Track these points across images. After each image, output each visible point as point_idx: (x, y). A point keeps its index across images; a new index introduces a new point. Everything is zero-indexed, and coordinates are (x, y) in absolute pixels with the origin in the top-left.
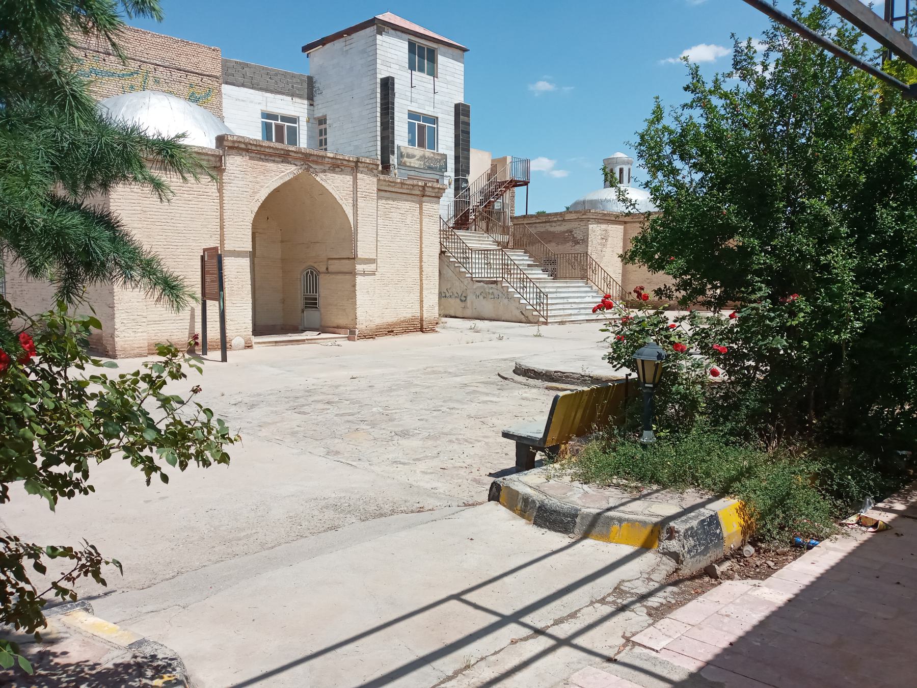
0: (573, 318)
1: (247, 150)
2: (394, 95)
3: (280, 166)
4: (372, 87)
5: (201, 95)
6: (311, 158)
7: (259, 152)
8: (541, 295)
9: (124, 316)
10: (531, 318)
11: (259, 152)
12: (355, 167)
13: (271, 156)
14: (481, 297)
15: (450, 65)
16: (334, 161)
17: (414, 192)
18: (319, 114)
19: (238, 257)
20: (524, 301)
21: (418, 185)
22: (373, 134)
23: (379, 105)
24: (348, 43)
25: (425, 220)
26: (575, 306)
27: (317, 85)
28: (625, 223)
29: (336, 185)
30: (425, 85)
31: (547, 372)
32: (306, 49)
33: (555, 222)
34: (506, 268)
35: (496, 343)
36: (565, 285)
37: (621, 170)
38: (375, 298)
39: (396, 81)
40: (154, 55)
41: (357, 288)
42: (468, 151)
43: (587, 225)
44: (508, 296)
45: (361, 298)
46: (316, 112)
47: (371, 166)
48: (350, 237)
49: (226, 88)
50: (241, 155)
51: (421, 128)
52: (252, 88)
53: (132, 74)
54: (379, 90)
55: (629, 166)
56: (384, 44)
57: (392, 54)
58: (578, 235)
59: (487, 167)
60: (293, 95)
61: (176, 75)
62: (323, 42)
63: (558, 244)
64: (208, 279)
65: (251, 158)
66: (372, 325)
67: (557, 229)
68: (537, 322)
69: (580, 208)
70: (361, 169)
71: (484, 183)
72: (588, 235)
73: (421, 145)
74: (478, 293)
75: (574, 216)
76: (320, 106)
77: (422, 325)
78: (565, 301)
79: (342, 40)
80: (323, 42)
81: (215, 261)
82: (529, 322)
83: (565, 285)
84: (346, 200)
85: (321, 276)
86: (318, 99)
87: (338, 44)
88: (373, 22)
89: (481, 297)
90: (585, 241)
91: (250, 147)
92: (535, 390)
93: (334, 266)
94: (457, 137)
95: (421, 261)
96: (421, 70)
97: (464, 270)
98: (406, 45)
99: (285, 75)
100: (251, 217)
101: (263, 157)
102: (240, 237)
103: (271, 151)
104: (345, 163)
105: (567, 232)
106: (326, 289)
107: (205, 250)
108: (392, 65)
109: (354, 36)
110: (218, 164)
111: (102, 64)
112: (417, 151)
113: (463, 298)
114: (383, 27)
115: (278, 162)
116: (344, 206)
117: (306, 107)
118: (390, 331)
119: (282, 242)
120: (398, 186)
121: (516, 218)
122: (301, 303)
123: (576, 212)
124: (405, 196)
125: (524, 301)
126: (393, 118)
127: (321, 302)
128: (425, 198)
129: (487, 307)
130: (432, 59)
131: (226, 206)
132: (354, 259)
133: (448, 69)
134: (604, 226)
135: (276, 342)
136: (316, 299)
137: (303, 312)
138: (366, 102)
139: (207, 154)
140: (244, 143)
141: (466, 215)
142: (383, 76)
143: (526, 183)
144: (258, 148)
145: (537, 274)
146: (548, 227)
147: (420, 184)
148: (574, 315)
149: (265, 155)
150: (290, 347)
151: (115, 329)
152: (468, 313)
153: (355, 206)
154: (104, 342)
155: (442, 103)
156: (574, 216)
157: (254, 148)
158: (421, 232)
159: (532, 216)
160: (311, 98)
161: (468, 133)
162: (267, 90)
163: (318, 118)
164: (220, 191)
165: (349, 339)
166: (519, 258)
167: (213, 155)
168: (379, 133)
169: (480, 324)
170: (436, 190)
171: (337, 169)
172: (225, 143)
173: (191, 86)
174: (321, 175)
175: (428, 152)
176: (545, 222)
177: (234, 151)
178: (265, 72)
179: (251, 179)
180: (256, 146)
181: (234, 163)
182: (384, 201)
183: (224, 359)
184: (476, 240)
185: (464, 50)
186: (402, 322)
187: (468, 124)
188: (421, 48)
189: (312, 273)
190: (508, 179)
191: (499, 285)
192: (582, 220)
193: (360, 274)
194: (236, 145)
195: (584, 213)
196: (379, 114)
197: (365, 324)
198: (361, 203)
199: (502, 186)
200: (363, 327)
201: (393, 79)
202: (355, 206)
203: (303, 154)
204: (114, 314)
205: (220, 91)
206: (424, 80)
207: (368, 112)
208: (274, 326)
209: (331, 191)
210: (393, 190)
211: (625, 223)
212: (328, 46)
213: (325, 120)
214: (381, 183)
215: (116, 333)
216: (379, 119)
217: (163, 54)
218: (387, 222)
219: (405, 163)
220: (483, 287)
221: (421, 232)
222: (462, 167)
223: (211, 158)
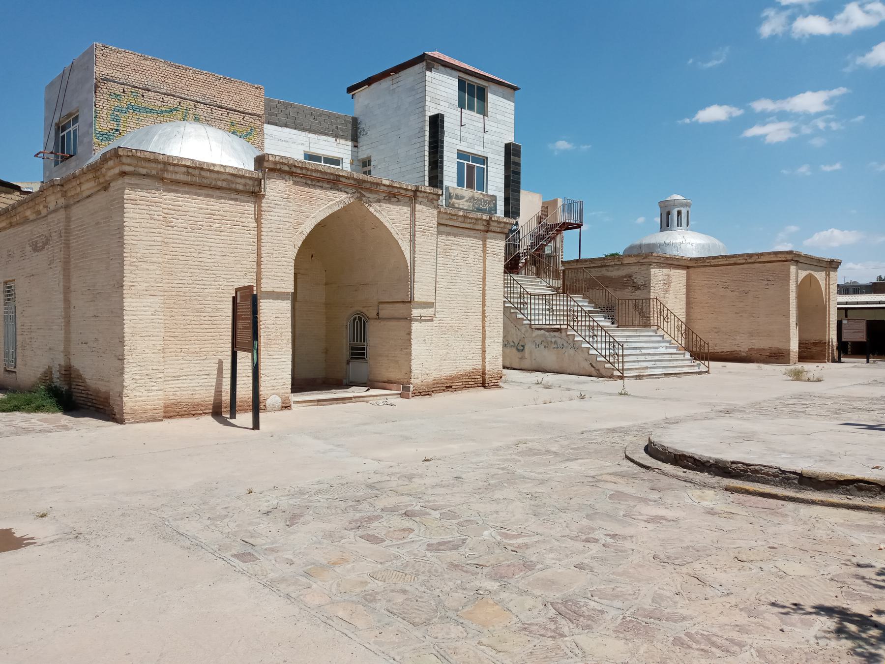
0: (649, 372)
1: (291, 174)
2: (443, 132)
3: (329, 193)
4: (421, 125)
5: (242, 125)
7: (305, 176)
8: (613, 344)
9: (136, 370)
10: (603, 372)
12: (413, 196)
13: (319, 181)
14: (542, 347)
15: (501, 104)
17: (477, 227)
18: (363, 155)
19: (277, 299)
20: (594, 352)
21: (481, 219)
22: (421, 174)
23: (427, 143)
24: (394, 81)
25: (489, 258)
26: (649, 358)
27: (362, 126)
28: (688, 267)
29: (392, 217)
30: (475, 123)
31: (717, 462)
32: (350, 90)
33: (612, 266)
34: (571, 315)
35: (577, 403)
36: (634, 334)
37: (679, 213)
38: (433, 347)
39: (445, 119)
40: (194, 92)
41: (413, 336)
42: (519, 192)
43: (648, 270)
44: (576, 346)
45: (417, 347)
46: (360, 154)
47: (431, 196)
48: (406, 278)
49: (268, 129)
50: (283, 178)
51: (470, 168)
52: (295, 129)
53: (171, 110)
54: (427, 128)
55: (688, 208)
56: (434, 81)
57: (441, 91)
58: (639, 280)
59: (537, 209)
60: (337, 136)
61: (217, 112)
62: (369, 82)
63: (615, 290)
64: (240, 325)
65: (295, 183)
66: (429, 380)
67: (615, 273)
68: (611, 376)
69: (635, 252)
70: (420, 199)
71: (534, 225)
72: (650, 280)
73: (470, 185)
74: (538, 342)
75: (633, 260)
76: (364, 148)
77: (484, 380)
78: (638, 352)
79: (388, 78)
80: (369, 82)
81: (249, 303)
82: (602, 377)
83: (634, 334)
85: (371, 322)
86: (363, 140)
87: (385, 83)
89: (542, 347)
90: (646, 286)
91: (294, 170)
92: (710, 493)
93: (386, 311)
94: (507, 178)
95: (484, 305)
96: (471, 108)
97: (521, 316)
98: (455, 83)
99: (329, 115)
100: (293, 252)
101: (309, 182)
102: (280, 276)
103: (319, 175)
104: (402, 192)
105: (625, 277)
106: (378, 337)
107: (237, 290)
108: (442, 103)
110: (257, 189)
111: (140, 99)
112: (466, 192)
113: (529, 350)
114: (431, 63)
115: (326, 189)
116: (400, 242)
117: (350, 148)
118: (448, 386)
119: (326, 284)
120: (460, 219)
121: (568, 262)
122: (346, 353)
123: (636, 256)
124: (467, 231)
125: (594, 352)
126: (442, 157)
127: (370, 352)
128: (489, 234)
129: (549, 357)
130: (482, 95)
131: (265, 239)
132: (410, 302)
133: (498, 107)
134: (666, 271)
135: (318, 401)
136: (363, 349)
137: (348, 363)
138: (414, 141)
139: (243, 177)
140: (288, 165)
141: (517, 259)
142: (432, 114)
143: (579, 226)
144: (304, 172)
145: (601, 320)
146: (604, 272)
147: (484, 217)
148: (651, 368)
149: (312, 180)
150: (334, 406)
151: (124, 387)
152: (526, 364)
153: (412, 241)
154: (112, 402)
155: (492, 143)
156: (633, 260)
157: (299, 171)
158: (484, 273)
159: (586, 260)
160: (355, 139)
161: (519, 173)
162: (310, 131)
163: (363, 159)
164: (258, 220)
165: (402, 396)
166: (581, 302)
167: (250, 178)
168: (427, 173)
169: (549, 378)
170: (502, 225)
171: (393, 199)
172: (266, 164)
173: (232, 124)
174: (375, 205)
175: (477, 194)
176: (601, 266)
177: (275, 175)
178: (308, 112)
179: (295, 208)
180: (301, 168)
181: (276, 189)
182: (444, 237)
183: (256, 426)
184: (534, 285)
185: (515, 89)
187: (519, 165)
188: (471, 86)
189: (360, 319)
190: (560, 219)
191: (564, 334)
192: (642, 264)
193: (417, 320)
194: (278, 167)
195: (645, 257)
196: (427, 153)
197: (421, 379)
198: (419, 239)
199: (551, 230)
200: (419, 382)
201: (442, 116)
202: (412, 241)
203: (355, 180)
204: (123, 368)
205: (262, 130)
206: (474, 118)
207: (416, 151)
208: (314, 380)
209: (386, 224)
211: (688, 267)
212: (374, 86)
213: (370, 161)
214: (442, 215)
215: (125, 391)
216: (427, 158)
217: (204, 91)
218: (447, 261)
219: (453, 204)
220: (543, 335)
221: (484, 273)
222: (512, 208)
223: (248, 181)
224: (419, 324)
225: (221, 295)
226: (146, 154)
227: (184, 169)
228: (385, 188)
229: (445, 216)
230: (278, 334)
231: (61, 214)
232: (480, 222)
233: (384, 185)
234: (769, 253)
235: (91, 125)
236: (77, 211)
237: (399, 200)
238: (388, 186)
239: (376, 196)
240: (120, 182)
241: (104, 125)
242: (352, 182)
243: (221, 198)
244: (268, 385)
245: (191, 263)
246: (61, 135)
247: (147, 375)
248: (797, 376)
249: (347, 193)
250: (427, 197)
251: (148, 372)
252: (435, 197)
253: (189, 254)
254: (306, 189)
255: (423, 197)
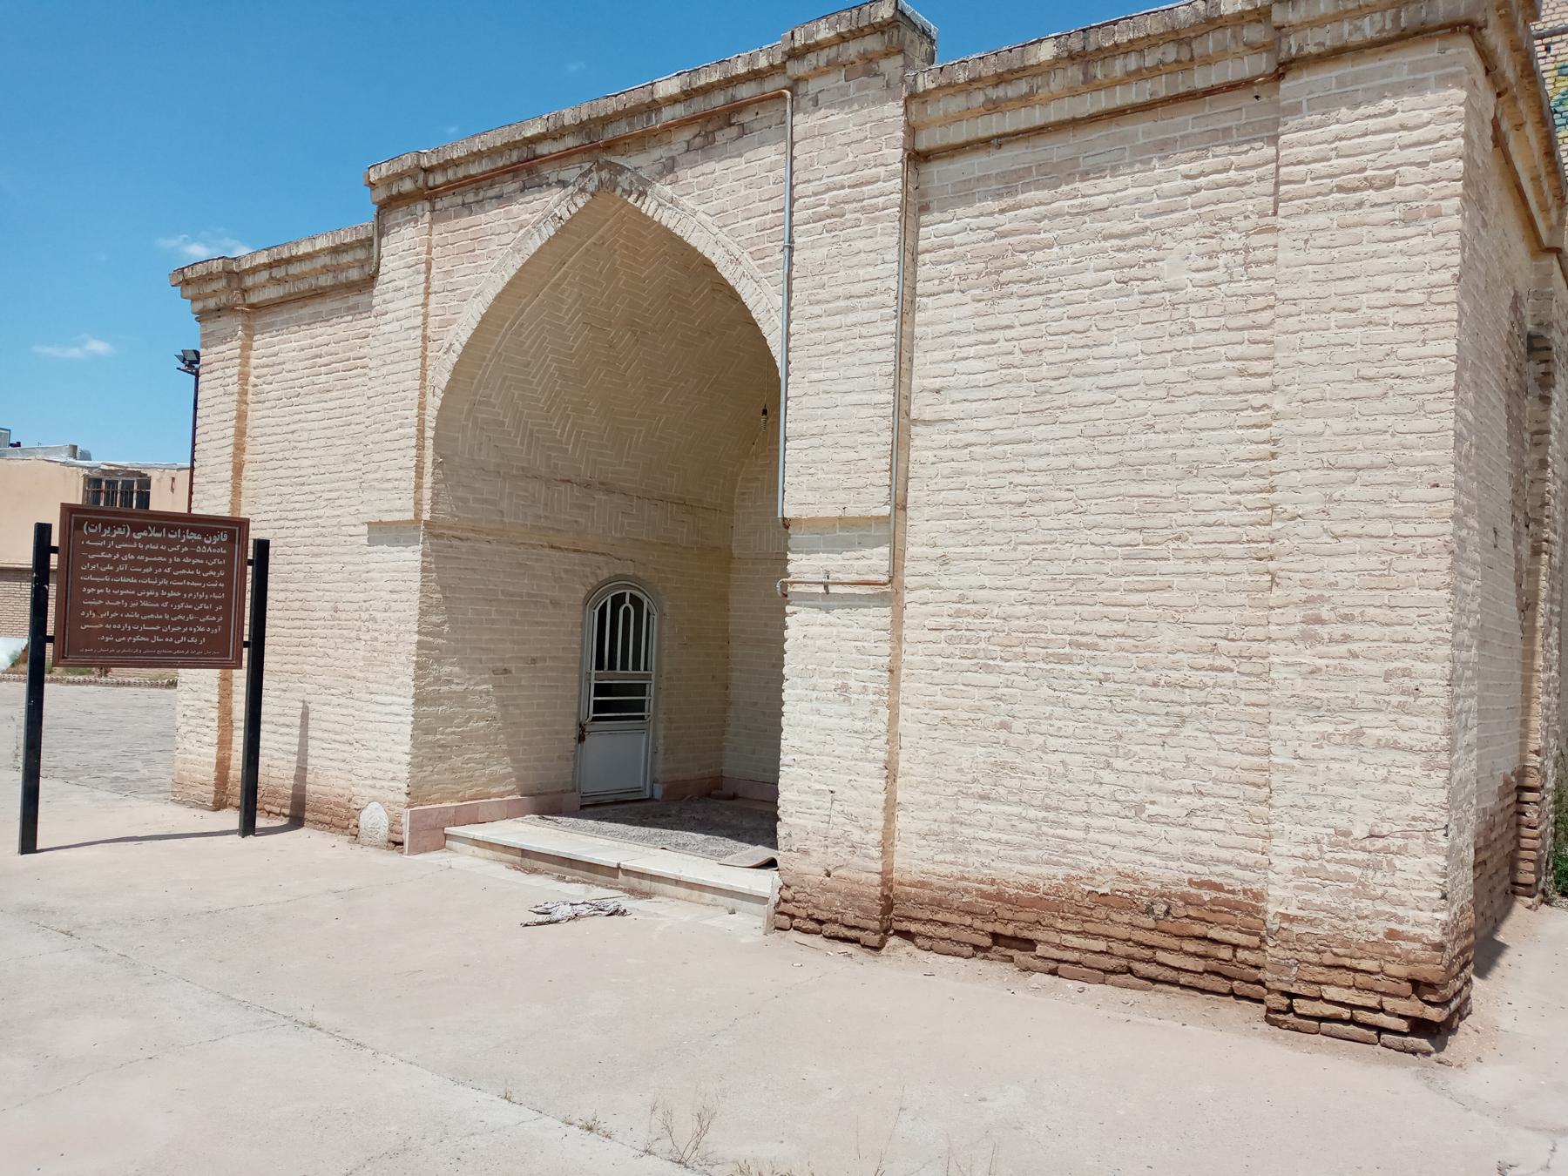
3: (515, 208)
6: (609, 134)
7: (453, 187)
11: (453, 187)
16: (699, 105)
65: (437, 216)
84: (759, 255)
103: (485, 166)
104: (745, 92)
120: (1057, 83)
124: (1140, 129)
135: (525, 853)
144: (450, 174)
157: (439, 179)
171: (721, 137)
186: (1124, 903)
210: (1037, 117)
214: (936, 110)
224: (821, 616)
225: (319, 540)
226: (198, 267)
227: (265, 275)
228: (679, 111)
229: (956, 104)
230: (392, 637)
232: (1211, 43)
233: (673, 100)
237: (744, 130)
238: (688, 95)
239: (660, 153)
242: (570, 142)
243: (334, 313)
244: (366, 773)
245: (282, 472)
247: (200, 710)
249: (563, 184)
250: (832, 65)
251: (199, 704)
252: (873, 43)
253: (280, 456)
254: (465, 221)
255: (818, 72)
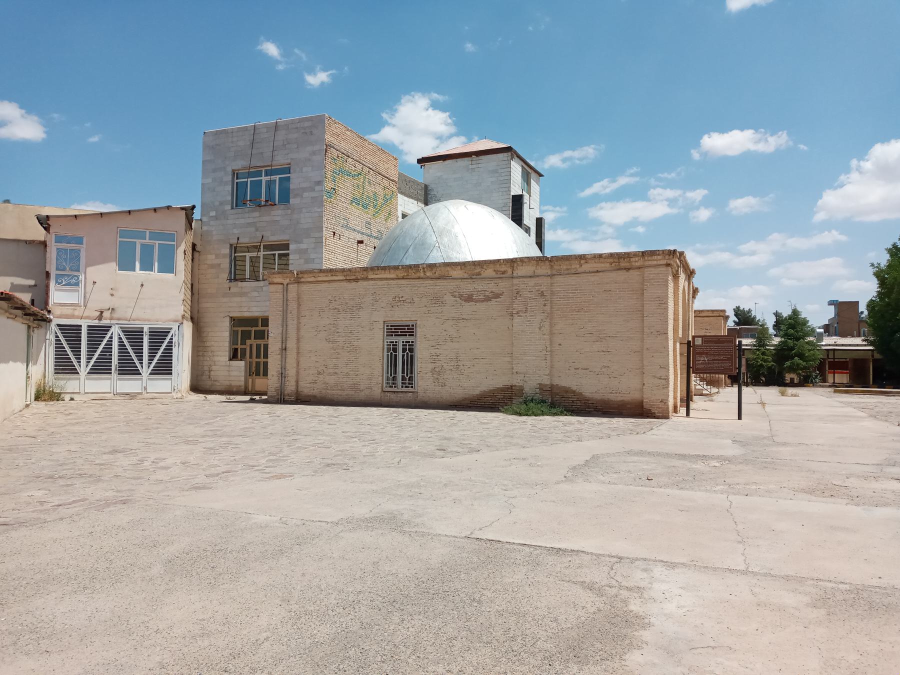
60: (417, 200)
61: (380, 177)
79: (470, 159)
88: (508, 149)
109: (481, 157)
154: (645, 406)
231: (547, 281)
234: (708, 311)
235: (320, 183)
236: (559, 279)
240: (663, 269)
241: (328, 185)
246: (236, 181)
248: (783, 394)
